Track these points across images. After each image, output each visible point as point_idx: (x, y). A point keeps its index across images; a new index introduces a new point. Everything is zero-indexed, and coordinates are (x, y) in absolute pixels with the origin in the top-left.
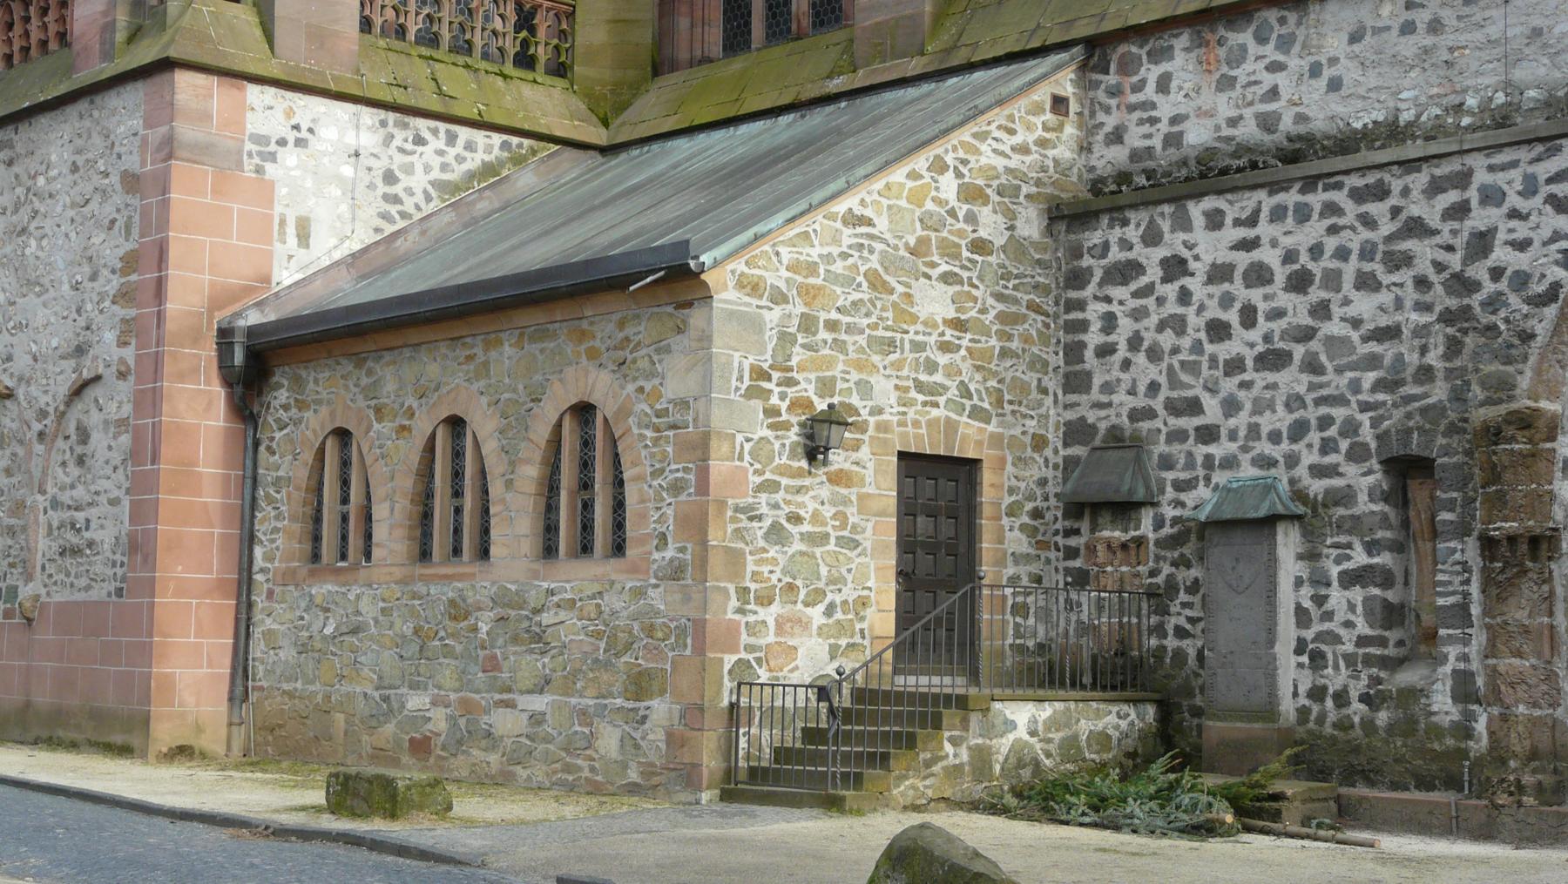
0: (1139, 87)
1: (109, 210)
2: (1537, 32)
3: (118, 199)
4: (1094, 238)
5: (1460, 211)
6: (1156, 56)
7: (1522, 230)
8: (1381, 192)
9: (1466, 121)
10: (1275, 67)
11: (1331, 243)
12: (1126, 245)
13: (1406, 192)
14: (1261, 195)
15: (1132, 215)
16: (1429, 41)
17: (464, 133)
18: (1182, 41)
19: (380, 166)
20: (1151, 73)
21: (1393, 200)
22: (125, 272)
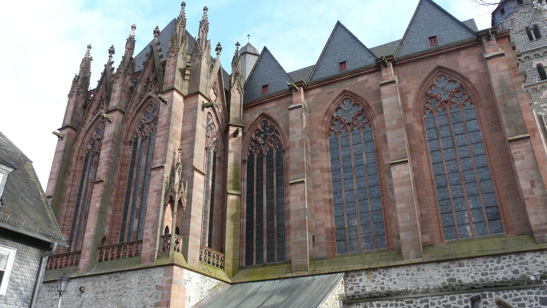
0: (356, 280)
1: (150, 293)
2: (431, 277)
3: (154, 291)
6: (358, 275)
8: (412, 302)
9: (420, 291)
10: (383, 279)
13: (416, 302)
14: (388, 301)
15: (361, 304)
16: (412, 277)
17: (212, 279)
19: (200, 286)
20: (358, 278)
21: (414, 304)
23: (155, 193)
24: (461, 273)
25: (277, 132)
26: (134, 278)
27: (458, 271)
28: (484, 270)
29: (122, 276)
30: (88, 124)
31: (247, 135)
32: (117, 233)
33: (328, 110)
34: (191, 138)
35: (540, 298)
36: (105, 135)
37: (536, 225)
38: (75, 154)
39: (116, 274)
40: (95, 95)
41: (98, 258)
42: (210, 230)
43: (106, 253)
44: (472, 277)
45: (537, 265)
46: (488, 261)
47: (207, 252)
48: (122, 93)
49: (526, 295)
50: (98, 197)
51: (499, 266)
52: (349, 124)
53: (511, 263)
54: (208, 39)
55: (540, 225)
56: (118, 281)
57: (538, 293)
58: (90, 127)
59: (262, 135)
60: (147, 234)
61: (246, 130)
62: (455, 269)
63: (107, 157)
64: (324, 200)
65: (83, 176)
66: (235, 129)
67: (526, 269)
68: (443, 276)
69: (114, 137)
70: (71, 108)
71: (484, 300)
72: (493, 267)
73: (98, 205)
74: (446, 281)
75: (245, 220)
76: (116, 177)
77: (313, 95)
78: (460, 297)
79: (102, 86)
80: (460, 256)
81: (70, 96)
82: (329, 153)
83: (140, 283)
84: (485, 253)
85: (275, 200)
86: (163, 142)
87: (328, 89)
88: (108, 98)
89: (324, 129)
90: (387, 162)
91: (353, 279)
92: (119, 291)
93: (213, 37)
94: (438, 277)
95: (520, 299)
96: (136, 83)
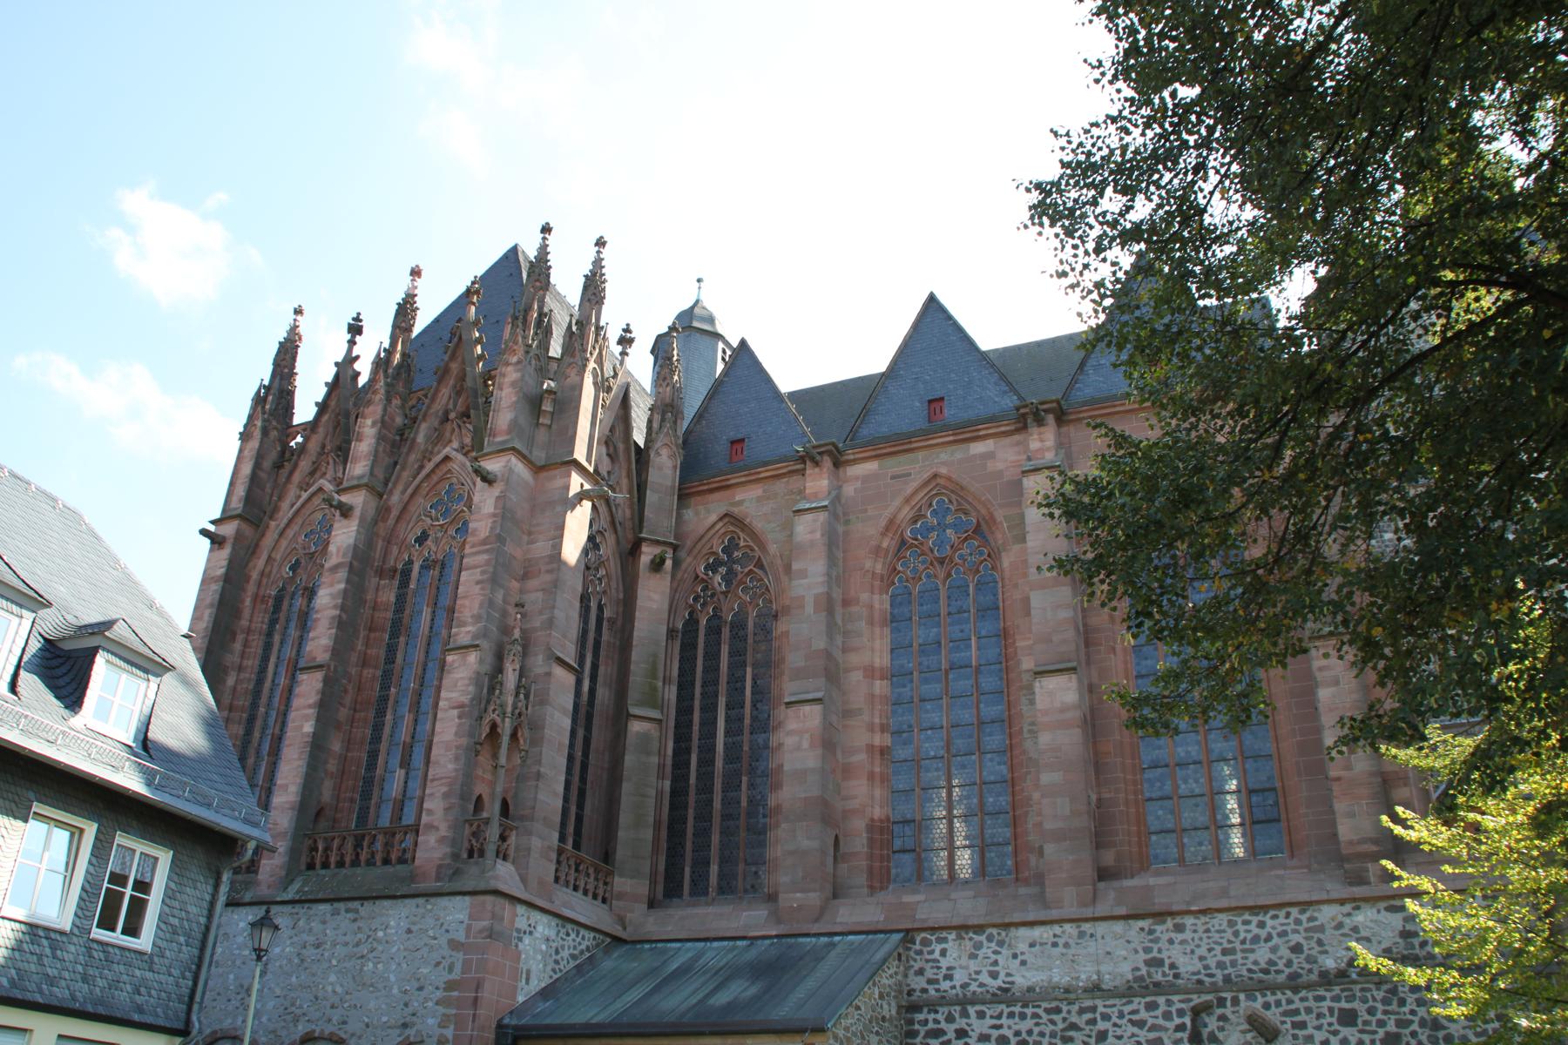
1: (436, 956)
3: (446, 952)
4: (921, 1017)
5: (1093, 1022)
7: (1119, 1032)
8: (1058, 1010)
10: (995, 952)
11: (1036, 1030)
12: (936, 1021)
13: (1069, 1012)
14: (1003, 1006)
15: (941, 1009)
17: (583, 932)
18: (952, 936)
20: (938, 948)
21: (1064, 1014)
22: (445, 990)
23: (455, 712)
24: (1176, 946)
25: (762, 567)
26: (395, 917)
27: (1171, 941)
28: (1230, 942)
29: (366, 909)
30: (286, 511)
31: (684, 566)
32: (352, 800)
33: (891, 522)
34: (548, 578)
35: (1340, 1010)
36: (332, 548)
37: (1351, 843)
38: (251, 588)
39: (351, 905)
40: (306, 439)
41: (304, 860)
42: (580, 806)
43: (326, 849)
44: (1201, 958)
45: (1343, 935)
46: (1239, 920)
47: (572, 862)
48: (378, 444)
49: (1311, 1003)
50: (310, 706)
51: (1263, 933)
52: (941, 561)
53: (1289, 928)
54: (602, 323)
55: (1360, 842)
56: (355, 920)
57: (1336, 999)
58: (290, 521)
59: (723, 570)
60: (430, 812)
61: (682, 554)
62: (1165, 937)
63: (335, 607)
64: (870, 748)
65: (268, 647)
66: (657, 550)
67: (1320, 943)
68: (1136, 952)
69: (355, 556)
70: (247, 469)
71: (1219, 1011)
72: (1249, 936)
73: (308, 728)
74: (1141, 965)
75: (667, 784)
76: (354, 658)
77: (857, 478)
78: (1169, 1003)
79: (325, 418)
80: (1175, 908)
81: (245, 436)
82: (887, 631)
83: (409, 931)
84: (1234, 904)
85: (746, 737)
86: (478, 583)
87: (896, 465)
88: (343, 453)
89: (879, 568)
90: (1027, 664)
91: (925, 950)
92: (357, 945)
93: (612, 317)
94: (1124, 953)
95: (1296, 1012)
96: (414, 420)
